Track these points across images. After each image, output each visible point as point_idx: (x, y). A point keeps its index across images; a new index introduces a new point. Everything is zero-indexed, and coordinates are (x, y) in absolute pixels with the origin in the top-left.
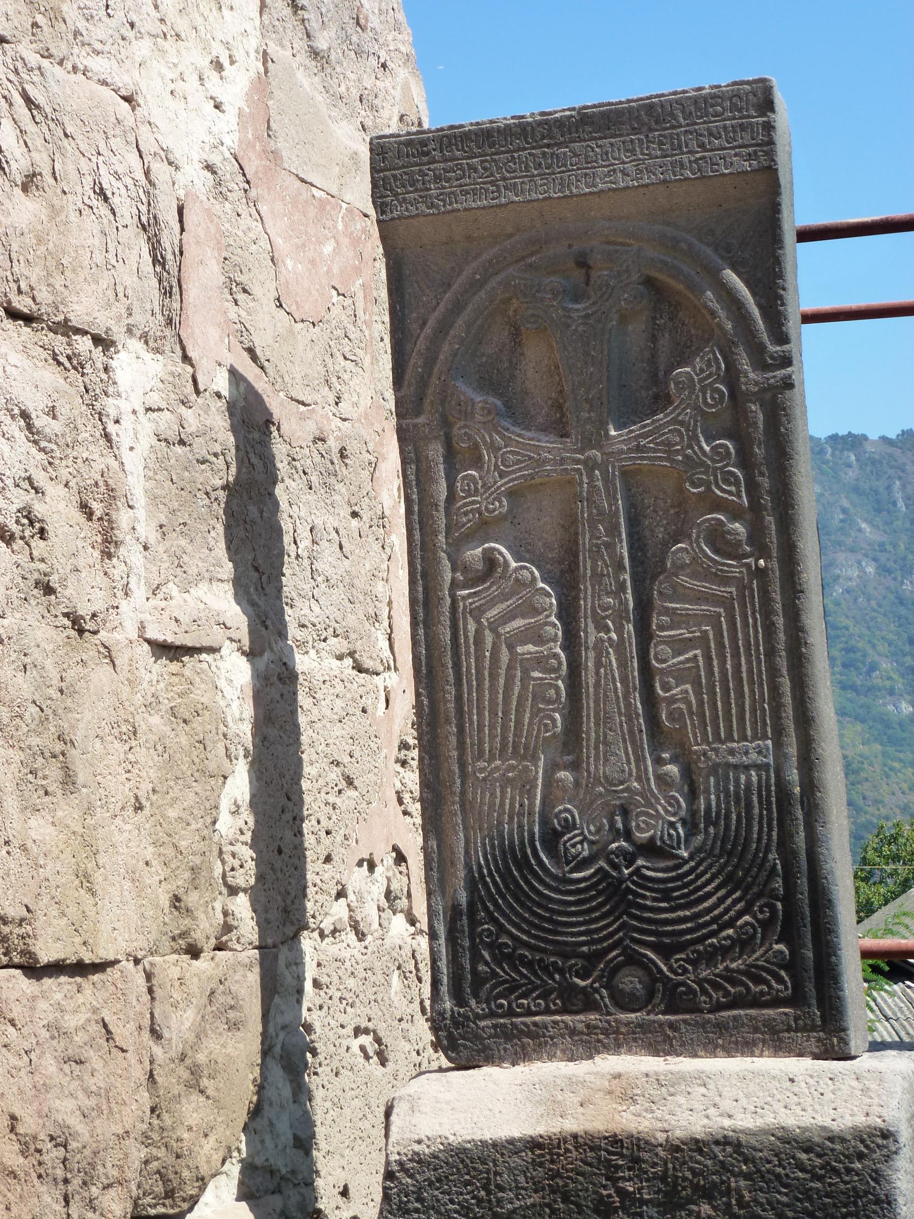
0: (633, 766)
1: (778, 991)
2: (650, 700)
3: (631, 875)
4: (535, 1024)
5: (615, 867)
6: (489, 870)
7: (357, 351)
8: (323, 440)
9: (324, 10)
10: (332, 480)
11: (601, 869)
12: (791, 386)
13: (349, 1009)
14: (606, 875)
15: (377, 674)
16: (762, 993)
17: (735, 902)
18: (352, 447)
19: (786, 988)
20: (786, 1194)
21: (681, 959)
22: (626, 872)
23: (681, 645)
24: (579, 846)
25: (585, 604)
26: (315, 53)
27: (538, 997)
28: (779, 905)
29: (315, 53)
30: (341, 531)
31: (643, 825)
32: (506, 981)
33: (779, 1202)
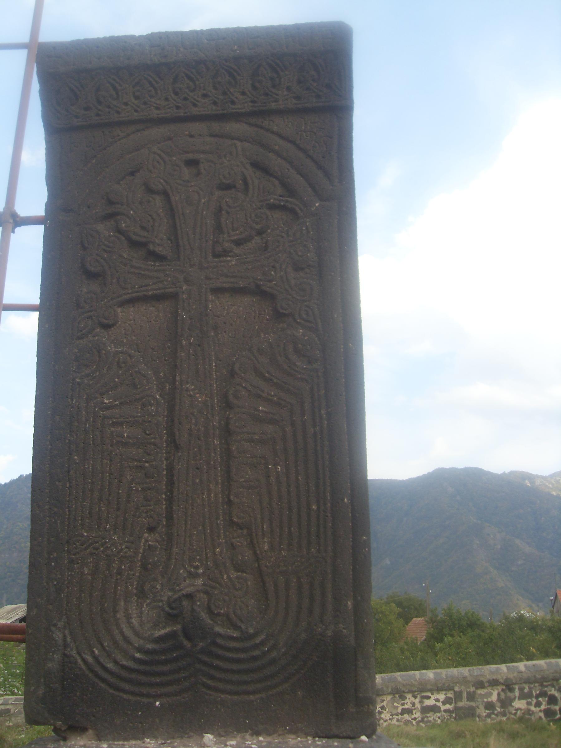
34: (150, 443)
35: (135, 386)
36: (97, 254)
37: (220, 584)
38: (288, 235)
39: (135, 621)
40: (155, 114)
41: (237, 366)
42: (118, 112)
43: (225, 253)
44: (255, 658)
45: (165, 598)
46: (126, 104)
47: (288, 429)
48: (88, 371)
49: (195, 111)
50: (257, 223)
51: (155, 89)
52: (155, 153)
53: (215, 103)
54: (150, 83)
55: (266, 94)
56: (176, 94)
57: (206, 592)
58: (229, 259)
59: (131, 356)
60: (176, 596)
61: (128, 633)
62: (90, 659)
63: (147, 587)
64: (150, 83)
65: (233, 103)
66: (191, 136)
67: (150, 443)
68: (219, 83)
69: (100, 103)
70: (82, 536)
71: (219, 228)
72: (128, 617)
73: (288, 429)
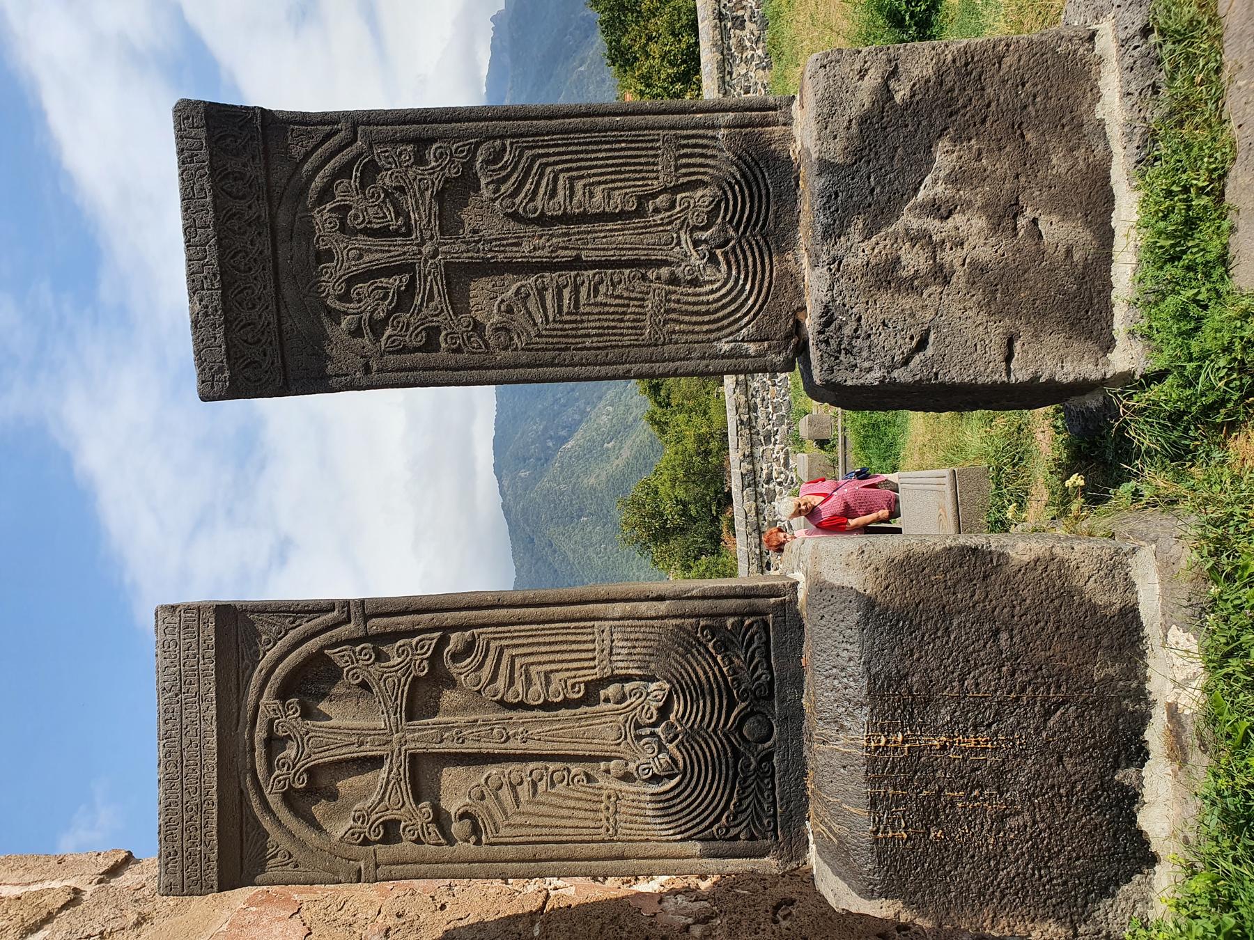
0: (608, 720)
1: (758, 627)
2: (567, 703)
3: (681, 725)
4: (781, 799)
5: (676, 736)
6: (676, 827)
7: (339, 900)
8: (389, 929)
9: (112, 916)
10: (416, 923)
11: (677, 746)
12: (363, 601)
13: (762, 927)
14: (681, 742)
15: (548, 896)
16: (760, 638)
17: (700, 653)
18: (397, 908)
19: (756, 622)
20: (904, 622)
21: (737, 693)
22: (679, 729)
23: (529, 682)
24: (662, 761)
25: (495, 748)
26: (138, 924)
27: (763, 796)
28: (702, 623)
29: (138, 924)
30: (449, 919)
31: (649, 715)
32: (752, 818)
33: (909, 627)
34: (575, 280)
35: (528, 295)
36: (411, 336)
37: (686, 219)
38: (391, 169)
39: (715, 286)
40: (271, 289)
41: (509, 211)
42: (269, 324)
43: (407, 223)
44: (741, 190)
45: (698, 262)
46: (260, 316)
47: (560, 167)
48: (516, 337)
49: (268, 252)
50: (379, 196)
51: (245, 288)
52: (309, 291)
53: (259, 234)
54: (239, 293)
55: (250, 186)
56: (250, 269)
57: (692, 231)
58: (413, 222)
59: (502, 301)
60: (695, 254)
61: (724, 291)
62: (746, 319)
63: (689, 278)
64: (239, 293)
65: (259, 217)
66: (291, 259)
67: (575, 280)
68: (239, 228)
69: (259, 340)
70: (650, 332)
71: (384, 232)
72: (712, 292)
73: (560, 167)
